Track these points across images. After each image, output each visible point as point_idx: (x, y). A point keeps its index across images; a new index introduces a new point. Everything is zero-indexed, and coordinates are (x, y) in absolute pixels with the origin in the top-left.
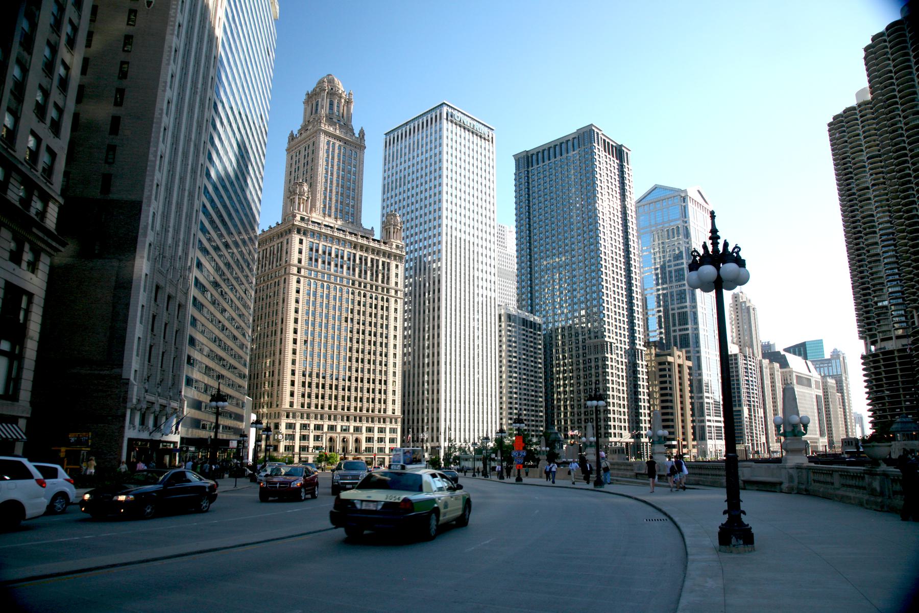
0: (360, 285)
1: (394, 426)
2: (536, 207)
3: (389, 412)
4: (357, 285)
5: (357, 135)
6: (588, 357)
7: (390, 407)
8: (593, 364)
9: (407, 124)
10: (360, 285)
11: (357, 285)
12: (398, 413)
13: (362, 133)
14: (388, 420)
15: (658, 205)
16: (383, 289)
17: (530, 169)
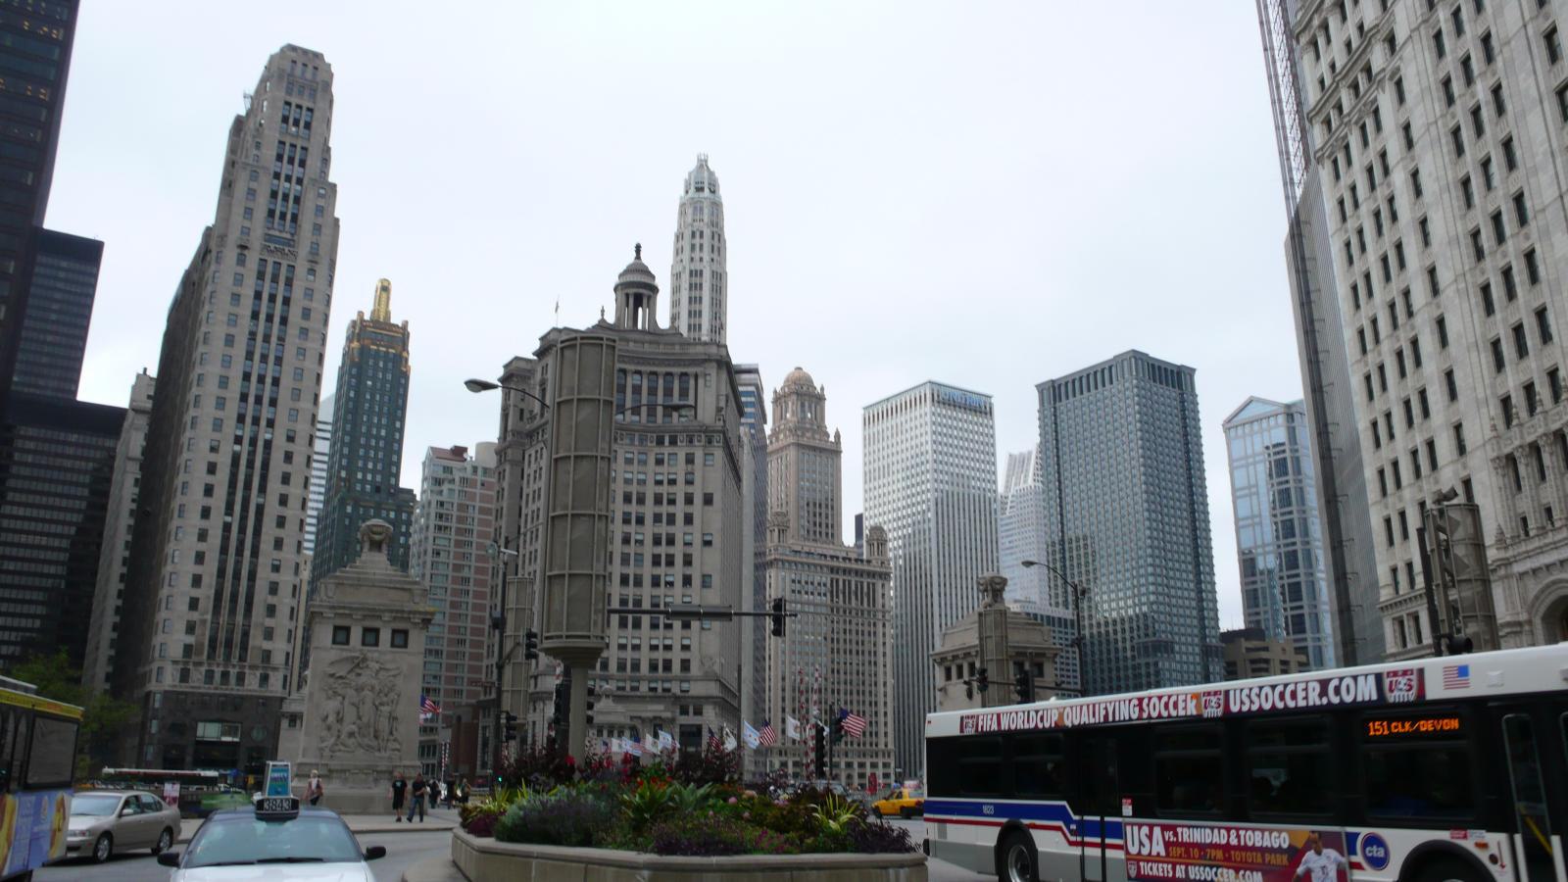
0: (845, 612)
1: (887, 760)
2: (1067, 466)
3: (882, 746)
4: (841, 612)
5: (832, 439)
6: (1138, 661)
7: (882, 740)
8: (1143, 671)
9: (888, 399)
10: (845, 612)
11: (841, 612)
12: (891, 746)
13: (838, 436)
14: (880, 754)
15: (1256, 426)
16: (869, 612)
17: (1058, 404)
